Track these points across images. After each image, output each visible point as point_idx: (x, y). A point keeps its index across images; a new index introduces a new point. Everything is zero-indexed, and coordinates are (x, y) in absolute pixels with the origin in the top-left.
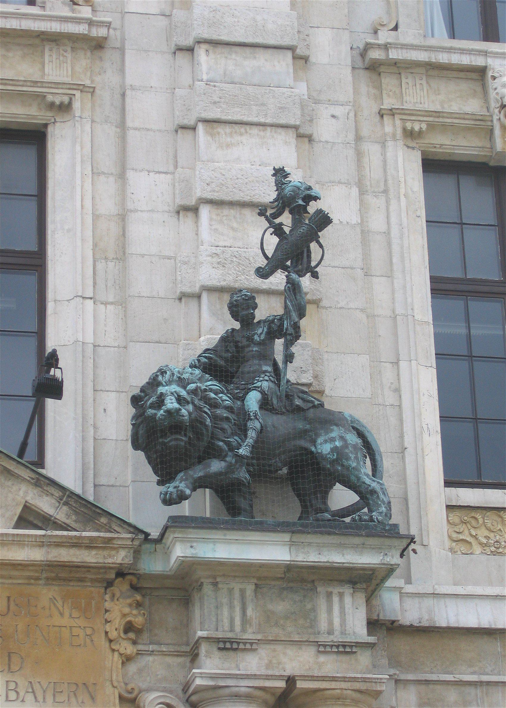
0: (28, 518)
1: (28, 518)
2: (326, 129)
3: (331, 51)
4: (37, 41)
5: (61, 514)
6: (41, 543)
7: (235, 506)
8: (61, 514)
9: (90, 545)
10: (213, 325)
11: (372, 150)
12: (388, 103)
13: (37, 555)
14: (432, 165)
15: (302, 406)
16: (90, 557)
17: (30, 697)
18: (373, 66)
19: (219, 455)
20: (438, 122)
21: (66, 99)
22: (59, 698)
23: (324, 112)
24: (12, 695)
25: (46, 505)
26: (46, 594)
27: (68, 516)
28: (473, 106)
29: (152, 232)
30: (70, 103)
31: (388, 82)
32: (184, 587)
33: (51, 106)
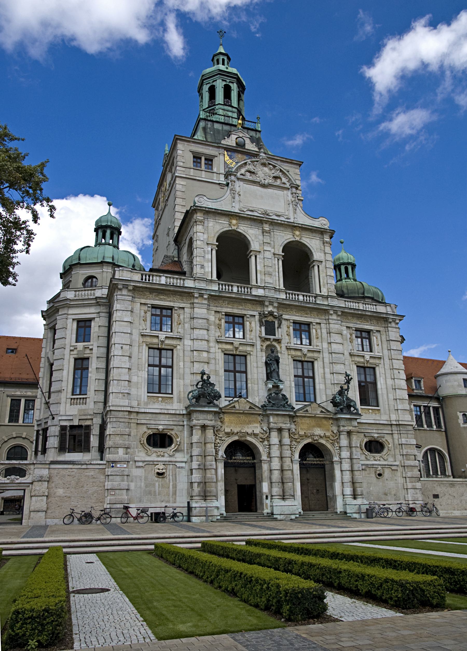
1: (322, 412)
2: (346, 363)
3: (347, 353)
5: (325, 411)
7: (341, 411)
8: (325, 411)
10: (338, 389)
11: (351, 365)
12: (353, 360)
13: (323, 416)
14: (357, 366)
15: (348, 399)
16: (328, 416)
18: (351, 355)
19: (342, 405)
20: (359, 362)
23: (346, 361)
25: (323, 410)
26: (323, 420)
28: (362, 360)
29: (328, 376)
31: (353, 357)
32: (337, 419)
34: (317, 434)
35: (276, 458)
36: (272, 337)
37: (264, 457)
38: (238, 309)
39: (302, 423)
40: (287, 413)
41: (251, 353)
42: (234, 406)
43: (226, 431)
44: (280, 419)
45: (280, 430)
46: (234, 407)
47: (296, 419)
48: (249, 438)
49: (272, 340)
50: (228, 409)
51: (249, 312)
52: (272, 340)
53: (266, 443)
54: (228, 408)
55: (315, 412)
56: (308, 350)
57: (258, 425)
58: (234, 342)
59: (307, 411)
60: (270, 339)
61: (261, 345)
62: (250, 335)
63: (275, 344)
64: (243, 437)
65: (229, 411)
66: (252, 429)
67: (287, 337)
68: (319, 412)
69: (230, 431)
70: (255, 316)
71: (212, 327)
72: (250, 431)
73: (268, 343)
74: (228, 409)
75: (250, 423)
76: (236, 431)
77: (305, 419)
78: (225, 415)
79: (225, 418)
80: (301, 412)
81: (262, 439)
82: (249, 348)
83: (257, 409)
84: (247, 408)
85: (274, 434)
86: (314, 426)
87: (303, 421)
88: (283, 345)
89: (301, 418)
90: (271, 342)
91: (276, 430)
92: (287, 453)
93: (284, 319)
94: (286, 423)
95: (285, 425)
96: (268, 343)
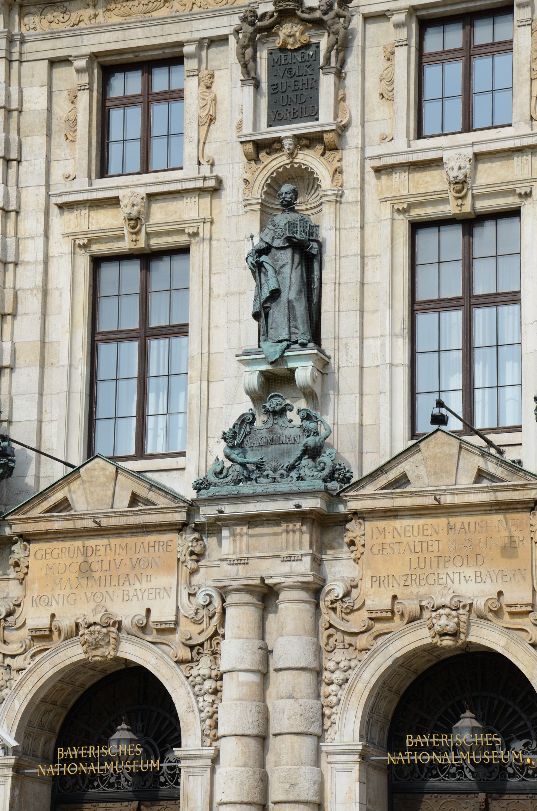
0: (481, 475)
1: (481, 475)
4: (510, 153)
6: (487, 490)
9: (515, 488)
17: (488, 580)
21: (528, 190)
22: (505, 579)
24: (479, 579)
27: (502, 473)
30: (531, 192)
33: (520, 195)
34: (446, 601)
35: (233, 740)
36: (286, 131)
37: (191, 739)
38: (144, 24)
39: (381, 550)
40: (288, 506)
41: (204, 230)
42: (65, 500)
43: (31, 623)
44: (267, 539)
45: (266, 596)
46: (64, 505)
47: (354, 529)
48: (134, 652)
49: (288, 144)
50: (37, 519)
51: (197, 25)
52: (288, 144)
53: (204, 666)
54: (37, 512)
55: (447, 482)
56: (478, 157)
57: (169, 580)
58: (120, 193)
59: (403, 480)
60: (279, 140)
61: (246, 181)
62: (202, 143)
63: (309, 159)
64: (97, 646)
65: (42, 526)
66: (139, 602)
67: (378, 110)
68: (466, 480)
69: (45, 622)
70: (223, 40)
71: (34, 146)
72: (128, 612)
73: (276, 162)
74: (37, 519)
75: (139, 569)
76: (65, 622)
77: (398, 523)
78: (33, 547)
79: (32, 562)
80: (370, 489)
81: (192, 647)
82: (188, 210)
83: (162, 501)
84: (122, 503)
85: (240, 617)
86: (443, 560)
87: (389, 539)
88: (350, 158)
89: (381, 524)
90: (291, 155)
91: (246, 598)
92: (288, 710)
93: (367, 18)
94: (289, 559)
95: (286, 568)
96: (276, 162)
